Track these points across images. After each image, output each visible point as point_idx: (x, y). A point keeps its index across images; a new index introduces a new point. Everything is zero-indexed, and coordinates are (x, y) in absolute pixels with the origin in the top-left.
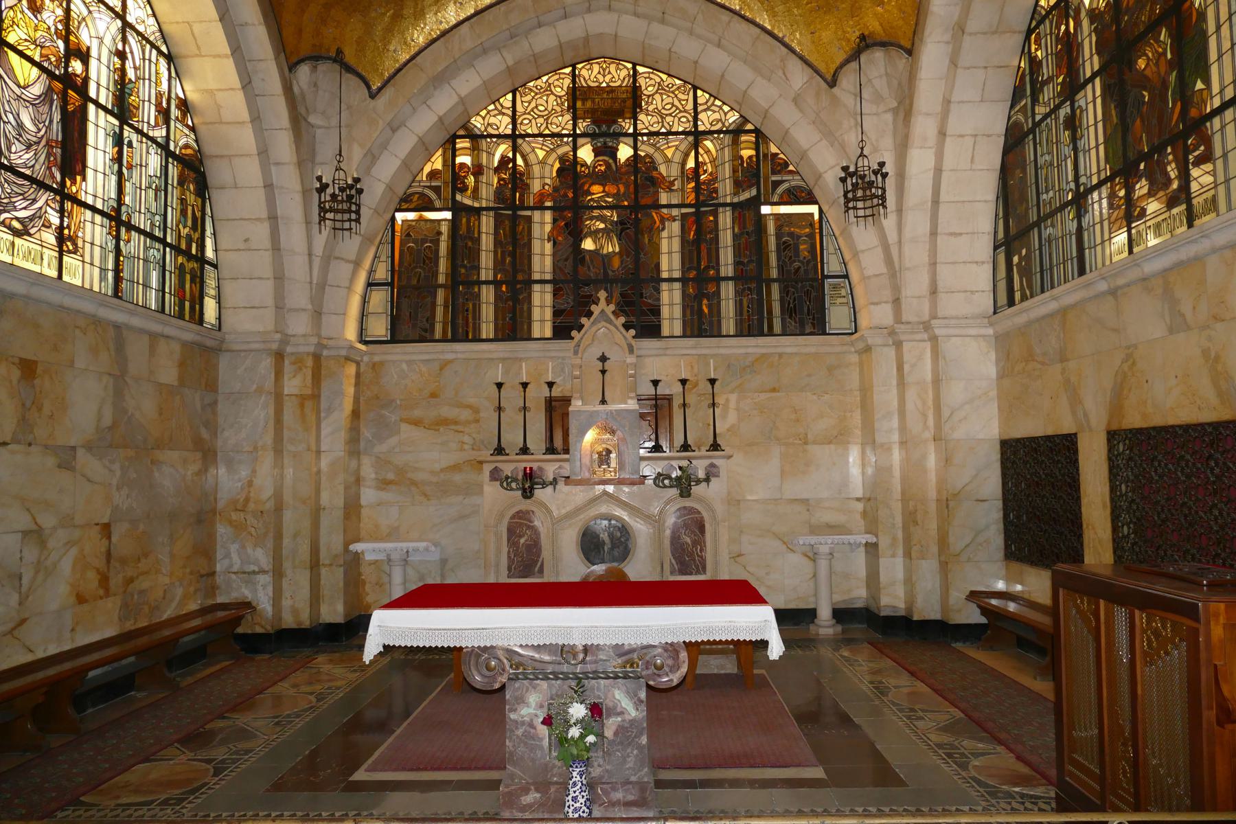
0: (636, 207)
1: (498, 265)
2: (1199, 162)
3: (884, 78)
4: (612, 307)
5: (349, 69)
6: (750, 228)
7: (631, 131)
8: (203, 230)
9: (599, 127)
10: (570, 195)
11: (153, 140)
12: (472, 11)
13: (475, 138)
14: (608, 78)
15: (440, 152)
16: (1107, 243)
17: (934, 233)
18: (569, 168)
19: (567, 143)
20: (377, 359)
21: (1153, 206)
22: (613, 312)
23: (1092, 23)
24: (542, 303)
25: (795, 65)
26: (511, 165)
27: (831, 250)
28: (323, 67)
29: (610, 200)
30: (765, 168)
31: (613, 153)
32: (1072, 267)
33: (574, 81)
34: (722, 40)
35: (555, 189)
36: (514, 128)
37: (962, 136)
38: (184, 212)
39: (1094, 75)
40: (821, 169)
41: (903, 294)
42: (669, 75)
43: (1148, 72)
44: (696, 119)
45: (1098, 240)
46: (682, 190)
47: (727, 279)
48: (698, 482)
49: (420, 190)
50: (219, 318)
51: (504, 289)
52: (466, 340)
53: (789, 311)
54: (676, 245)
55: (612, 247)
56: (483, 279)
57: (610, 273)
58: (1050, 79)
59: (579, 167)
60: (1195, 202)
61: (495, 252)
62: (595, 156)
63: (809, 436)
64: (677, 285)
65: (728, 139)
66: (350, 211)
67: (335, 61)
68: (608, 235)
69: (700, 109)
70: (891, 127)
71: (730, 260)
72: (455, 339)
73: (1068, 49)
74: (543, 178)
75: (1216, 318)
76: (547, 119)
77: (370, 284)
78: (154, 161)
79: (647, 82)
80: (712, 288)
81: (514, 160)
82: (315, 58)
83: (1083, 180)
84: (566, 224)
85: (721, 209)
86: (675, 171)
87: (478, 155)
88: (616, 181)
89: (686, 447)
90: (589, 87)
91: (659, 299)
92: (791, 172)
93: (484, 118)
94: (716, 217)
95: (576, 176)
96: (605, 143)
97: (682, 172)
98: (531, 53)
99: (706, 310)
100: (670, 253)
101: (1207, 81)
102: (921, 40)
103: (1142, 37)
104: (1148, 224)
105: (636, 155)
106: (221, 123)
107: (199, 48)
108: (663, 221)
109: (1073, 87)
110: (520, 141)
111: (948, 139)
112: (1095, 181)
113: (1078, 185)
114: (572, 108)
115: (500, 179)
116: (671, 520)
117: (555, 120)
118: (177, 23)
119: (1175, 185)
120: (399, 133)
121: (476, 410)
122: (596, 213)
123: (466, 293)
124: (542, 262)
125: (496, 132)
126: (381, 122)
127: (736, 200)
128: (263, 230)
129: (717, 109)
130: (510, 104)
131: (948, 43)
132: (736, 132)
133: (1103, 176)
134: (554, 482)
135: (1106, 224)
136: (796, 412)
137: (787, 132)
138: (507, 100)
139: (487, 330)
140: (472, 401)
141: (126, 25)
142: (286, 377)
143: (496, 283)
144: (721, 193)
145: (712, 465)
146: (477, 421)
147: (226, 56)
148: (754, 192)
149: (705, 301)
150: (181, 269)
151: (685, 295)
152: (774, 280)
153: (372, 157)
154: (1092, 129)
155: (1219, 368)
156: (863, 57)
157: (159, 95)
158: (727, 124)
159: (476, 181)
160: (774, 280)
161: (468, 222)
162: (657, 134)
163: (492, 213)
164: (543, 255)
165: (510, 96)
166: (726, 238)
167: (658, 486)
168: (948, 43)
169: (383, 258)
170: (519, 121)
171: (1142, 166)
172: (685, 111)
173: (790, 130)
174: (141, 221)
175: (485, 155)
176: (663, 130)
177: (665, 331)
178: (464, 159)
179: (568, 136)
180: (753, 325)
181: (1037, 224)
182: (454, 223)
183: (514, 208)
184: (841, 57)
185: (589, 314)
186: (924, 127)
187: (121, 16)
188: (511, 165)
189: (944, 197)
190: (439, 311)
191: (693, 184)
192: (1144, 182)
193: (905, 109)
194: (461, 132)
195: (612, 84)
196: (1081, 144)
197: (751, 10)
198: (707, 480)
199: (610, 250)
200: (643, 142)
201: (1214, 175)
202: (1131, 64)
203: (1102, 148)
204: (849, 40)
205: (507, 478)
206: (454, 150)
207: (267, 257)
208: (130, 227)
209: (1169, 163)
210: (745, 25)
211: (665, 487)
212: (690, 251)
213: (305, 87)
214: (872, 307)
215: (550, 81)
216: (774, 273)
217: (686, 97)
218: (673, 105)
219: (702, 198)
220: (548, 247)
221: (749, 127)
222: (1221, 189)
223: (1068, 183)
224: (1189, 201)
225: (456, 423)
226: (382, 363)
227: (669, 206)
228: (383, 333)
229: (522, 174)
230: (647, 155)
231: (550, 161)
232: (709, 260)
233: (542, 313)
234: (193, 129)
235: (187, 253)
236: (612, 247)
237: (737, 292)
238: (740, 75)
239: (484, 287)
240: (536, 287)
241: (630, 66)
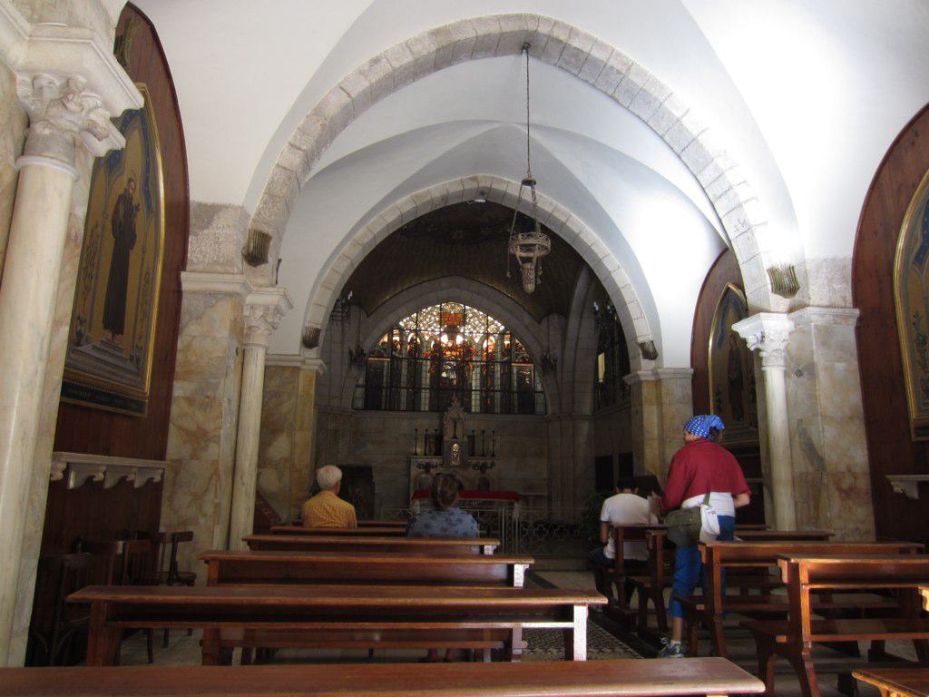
0: (463, 361)
1: (408, 381)
13: (401, 330)
24: (425, 396)
25: (525, 314)
30: (513, 349)
55: (453, 376)
64: (478, 393)
71: (499, 383)
72: (391, 410)
91: (470, 398)
95: (441, 347)
108: (474, 367)
109: (612, 343)
116: (477, 482)
132: (502, 334)
139: (403, 407)
151: (481, 396)
156: (550, 316)
164: (426, 378)
177: (473, 410)
178: (396, 338)
185: (450, 405)
198: (491, 467)
216: (515, 389)
220: (429, 375)
236: (453, 376)
240: (423, 391)
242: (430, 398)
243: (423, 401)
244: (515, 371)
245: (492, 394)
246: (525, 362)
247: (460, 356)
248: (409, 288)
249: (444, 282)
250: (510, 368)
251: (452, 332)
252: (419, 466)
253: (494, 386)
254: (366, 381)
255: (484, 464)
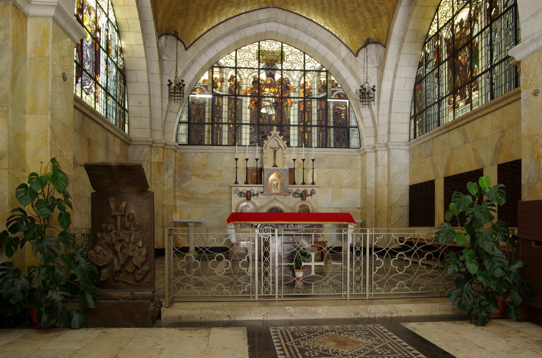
0: (281, 97)
1: (229, 118)
2: (474, 91)
3: (375, 55)
4: (279, 132)
5: (178, 39)
6: (323, 107)
7: (280, 68)
8: (125, 98)
9: (268, 66)
10: (257, 91)
11: (114, 62)
12: (224, 19)
13: (221, 67)
14: (272, 48)
15: (207, 72)
16: (447, 116)
17: (390, 112)
18: (257, 82)
19: (256, 72)
20: (183, 151)
21: (461, 104)
22: (279, 134)
23: (445, 43)
24: (246, 132)
25: (343, 47)
26: (234, 79)
27: (352, 117)
28: (170, 38)
29: (272, 94)
30: (329, 86)
31: (273, 76)
32: (436, 124)
33: (259, 48)
34: (317, 37)
35: (252, 89)
36: (236, 65)
37: (401, 78)
38: (120, 91)
39: (446, 60)
40: (351, 87)
41: (378, 133)
42: (295, 48)
43: (462, 61)
44: (304, 65)
45: (445, 115)
46: (299, 92)
47: (314, 126)
48: (308, 196)
49: (199, 87)
50: (128, 132)
51: (231, 126)
52: (217, 145)
53: (337, 139)
54: (296, 112)
55: (272, 112)
56: (224, 122)
57: (272, 122)
58: (432, 60)
59: (260, 81)
60: (473, 103)
61: (228, 112)
62: (267, 77)
63: (342, 185)
64: (296, 128)
65: (316, 74)
66: (180, 93)
67: (174, 35)
68: (271, 107)
69: (306, 61)
70: (376, 73)
71: (316, 119)
72: (212, 145)
73: (438, 50)
74: (247, 84)
75: (477, 139)
76: (248, 62)
77: (180, 123)
78: (114, 70)
79: (287, 49)
80: (309, 129)
81: (236, 77)
82: (167, 34)
83: (441, 95)
84: (255, 103)
85: (313, 100)
86: (296, 85)
87: (222, 75)
88: (274, 87)
89: (303, 183)
90: (265, 50)
92: (339, 87)
93: (224, 60)
94: (311, 103)
95: (259, 84)
96: (270, 72)
97: (299, 85)
98: (245, 36)
99: (306, 137)
100: (294, 115)
101: (478, 66)
102: (389, 43)
103: (460, 49)
104: (460, 109)
105: (282, 78)
106: (134, 57)
107: (129, 29)
108: (292, 103)
109: (439, 63)
110: (238, 70)
111: (397, 79)
112: (444, 95)
113: (439, 97)
114: (259, 58)
115: (230, 84)
117: (252, 63)
118: (123, 19)
119: (468, 97)
120: (194, 64)
121: (221, 172)
122: (267, 99)
123: (217, 127)
124: (246, 117)
125: (229, 66)
126: (189, 60)
127: (318, 97)
128: (146, 99)
129: (312, 62)
130: (235, 56)
131: (398, 44)
132: (320, 71)
133: (447, 94)
134: (257, 194)
135: (447, 109)
136: (338, 176)
137: (339, 72)
138: (233, 54)
140: (219, 168)
141: (109, 20)
142: (153, 155)
143: (228, 124)
144: (313, 94)
145: (313, 190)
146: (221, 176)
147: (139, 32)
148: (325, 94)
149: (306, 134)
150: (120, 111)
151: (299, 131)
152: (332, 127)
153: (184, 73)
154: (444, 78)
155: (477, 153)
156: (369, 46)
157: (116, 46)
158: (316, 68)
159: (221, 85)
160: (332, 127)
161: (218, 99)
162: (290, 70)
163: (227, 97)
164: (246, 114)
165: (235, 52)
166: (315, 111)
167: (294, 197)
168: (398, 44)
169: (185, 113)
170: (238, 62)
171: (459, 91)
172: (301, 62)
173: (340, 72)
174: (112, 93)
175: (224, 74)
176: (292, 69)
178: (217, 75)
179: (257, 69)
180: (324, 144)
181: (425, 110)
182: (213, 100)
183: (236, 95)
184: (360, 46)
186: (388, 74)
187: (107, 16)
188: (234, 79)
189: (394, 99)
190: (206, 134)
191: (303, 90)
192: (459, 96)
193: (381, 67)
194: (216, 65)
195: (273, 50)
196: (441, 83)
197: (328, 26)
198: (311, 195)
199: (272, 113)
200: (285, 73)
201: (479, 95)
202: (457, 58)
203: (447, 84)
204: (363, 40)
205: (240, 192)
206: (213, 72)
207: (148, 109)
208: (110, 95)
209: (466, 90)
210: (325, 31)
211: (296, 197)
212: (301, 115)
213: (162, 45)
214: (367, 138)
215: (250, 47)
216: (332, 125)
217: (301, 57)
218: (296, 59)
219: (306, 95)
220: (248, 111)
221: (324, 69)
222: (480, 99)
223: (436, 96)
224: (471, 102)
225: (213, 176)
226: (185, 153)
227: (294, 98)
228: (185, 141)
229: (239, 83)
230: (286, 78)
231: (250, 78)
232: (308, 119)
233: (246, 136)
234: (123, 59)
235: (120, 106)
236: (272, 112)
237: (318, 131)
238: (323, 50)
239: (224, 125)
240: (244, 126)
241: (280, 43)
242: (251, 133)
243: (244, 136)
244: (331, 106)
245: (309, 129)
246: (341, 98)
247: (278, 93)
248: (226, 20)
249: (262, 15)
250: (327, 104)
251: (270, 69)
252: (240, 194)
253: (311, 122)
254: (189, 117)
255: (305, 192)
